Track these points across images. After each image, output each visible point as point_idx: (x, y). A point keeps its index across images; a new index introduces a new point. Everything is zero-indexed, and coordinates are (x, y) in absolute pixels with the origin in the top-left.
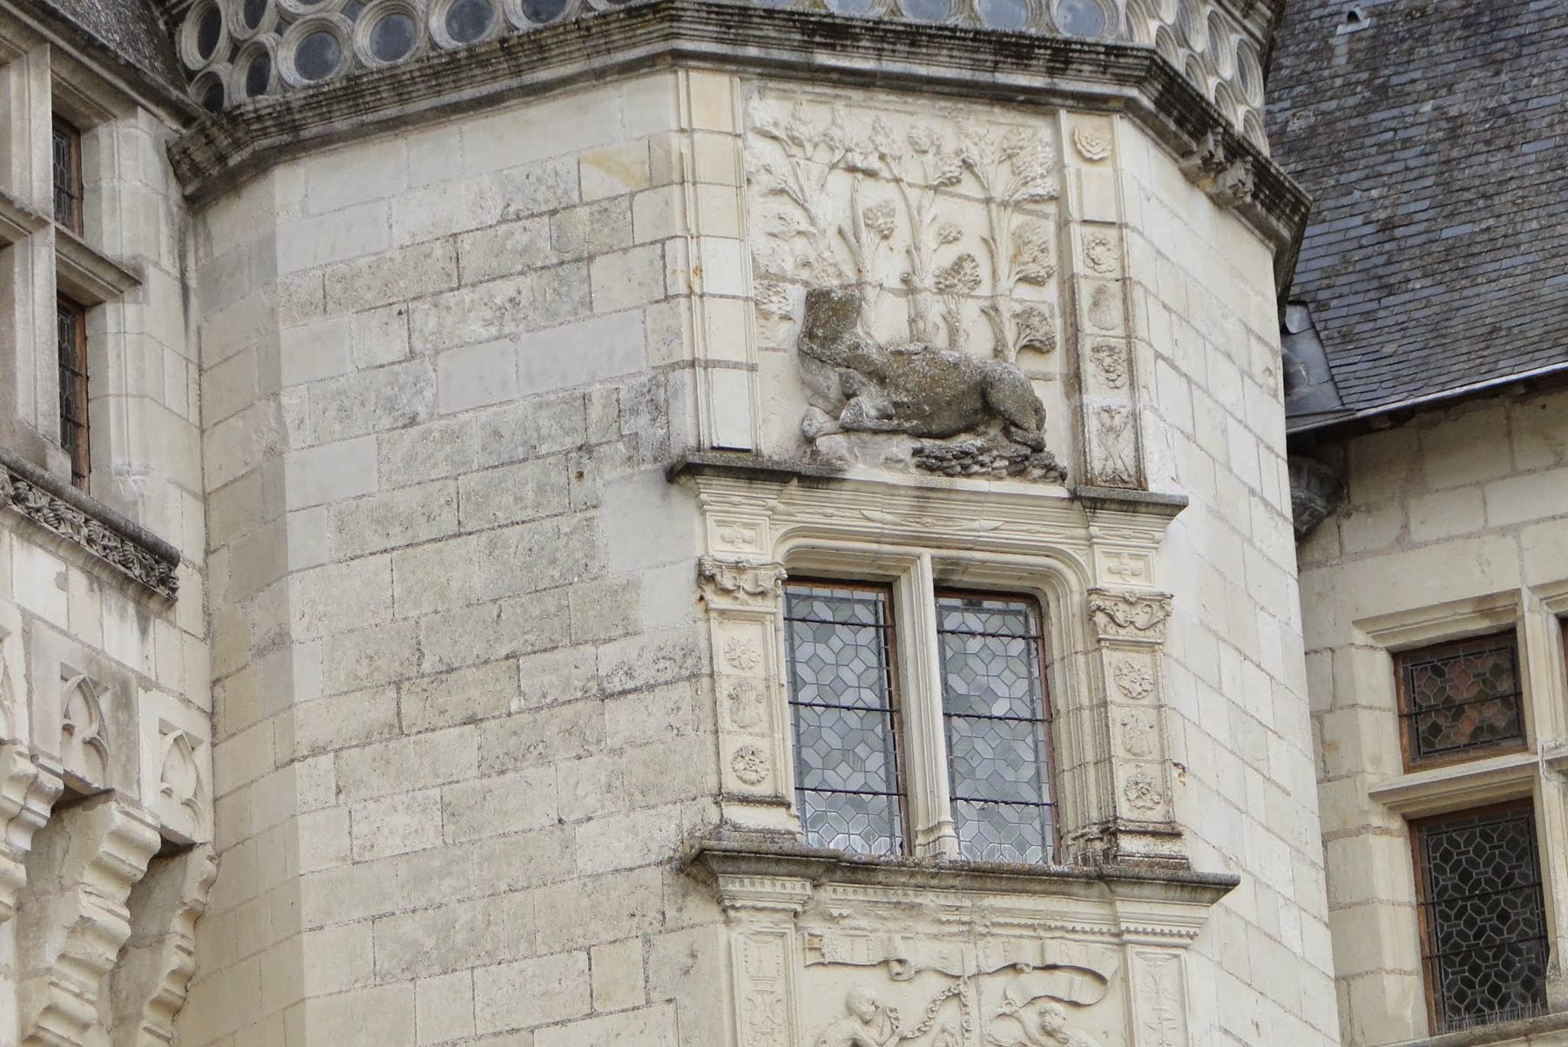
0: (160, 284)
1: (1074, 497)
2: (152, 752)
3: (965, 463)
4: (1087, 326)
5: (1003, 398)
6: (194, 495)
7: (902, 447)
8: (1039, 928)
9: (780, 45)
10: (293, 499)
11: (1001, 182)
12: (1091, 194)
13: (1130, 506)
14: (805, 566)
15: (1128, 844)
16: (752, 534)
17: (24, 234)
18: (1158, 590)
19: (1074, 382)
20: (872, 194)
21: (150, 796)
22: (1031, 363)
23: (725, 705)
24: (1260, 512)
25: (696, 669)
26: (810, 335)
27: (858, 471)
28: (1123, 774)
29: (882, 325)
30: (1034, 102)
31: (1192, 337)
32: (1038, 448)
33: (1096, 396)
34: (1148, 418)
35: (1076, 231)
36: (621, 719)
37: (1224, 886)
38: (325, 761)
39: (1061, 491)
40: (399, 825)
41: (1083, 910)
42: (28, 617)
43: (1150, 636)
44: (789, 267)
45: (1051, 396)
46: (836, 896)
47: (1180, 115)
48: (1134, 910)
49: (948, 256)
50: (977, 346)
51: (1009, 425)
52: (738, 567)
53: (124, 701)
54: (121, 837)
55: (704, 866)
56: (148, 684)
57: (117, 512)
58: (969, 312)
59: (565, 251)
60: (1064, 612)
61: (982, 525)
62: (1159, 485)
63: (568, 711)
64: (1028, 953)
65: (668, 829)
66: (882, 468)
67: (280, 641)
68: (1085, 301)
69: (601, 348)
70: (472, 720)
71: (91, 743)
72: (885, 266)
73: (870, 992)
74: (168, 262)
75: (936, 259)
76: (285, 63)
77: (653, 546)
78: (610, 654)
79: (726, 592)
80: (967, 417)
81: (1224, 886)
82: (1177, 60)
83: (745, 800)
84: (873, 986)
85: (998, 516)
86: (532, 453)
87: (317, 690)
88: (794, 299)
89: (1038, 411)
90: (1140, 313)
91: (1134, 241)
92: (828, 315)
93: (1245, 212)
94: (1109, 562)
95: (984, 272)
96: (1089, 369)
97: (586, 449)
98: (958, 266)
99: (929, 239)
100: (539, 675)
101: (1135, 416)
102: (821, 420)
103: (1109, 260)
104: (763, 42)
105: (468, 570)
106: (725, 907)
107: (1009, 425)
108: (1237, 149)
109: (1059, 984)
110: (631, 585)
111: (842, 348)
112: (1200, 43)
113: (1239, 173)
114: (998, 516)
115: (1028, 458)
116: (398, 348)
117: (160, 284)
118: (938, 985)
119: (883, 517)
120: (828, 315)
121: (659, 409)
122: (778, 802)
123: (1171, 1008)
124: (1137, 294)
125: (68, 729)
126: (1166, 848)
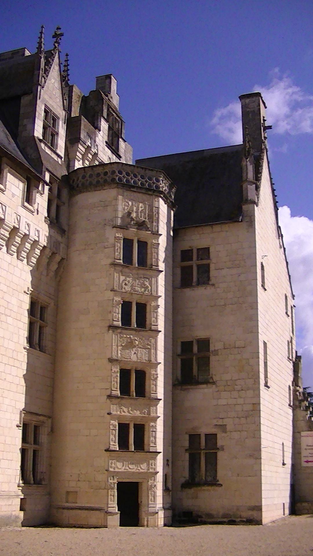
0: (66, 205)
13: (157, 234)
15: (154, 267)
78: (106, 244)
80: (141, 225)
85: (144, 235)
114: (144, 235)
115: (147, 229)
117: (66, 205)
121: (113, 221)
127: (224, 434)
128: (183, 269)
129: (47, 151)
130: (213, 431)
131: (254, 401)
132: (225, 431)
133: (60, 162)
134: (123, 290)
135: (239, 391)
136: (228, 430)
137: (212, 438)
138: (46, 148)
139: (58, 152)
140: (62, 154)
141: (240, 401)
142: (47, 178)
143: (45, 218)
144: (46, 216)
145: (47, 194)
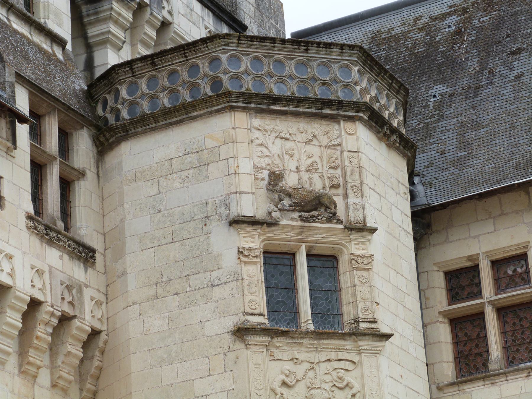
0: (91, 175)
1: (346, 227)
2: (88, 305)
3: (314, 219)
4: (349, 180)
5: (325, 201)
6: (101, 234)
7: (296, 215)
8: (337, 349)
10: (127, 234)
11: (325, 141)
12: (349, 143)
14: (271, 249)
15: (362, 325)
16: (254, 241)
17: (51, 162)
18: (370, 253)
19: (346, 196)
20: (289, 145)
21: (88, 317)
22: (333, 191)
23: (246, 288)
24: (403, 233)
25: (239, 279)
26: (269, 184)
27: (284, 222)
28: (360, 305)
29: (291, 181)
30: (334, 118)
31: (377, 183)
32: (335, 214)
33: (352, 199)
34: (367, 205)
35: (346, 154)
36: (217, 292)
37: (388, 336)
38: (136, 306)
39: (342, 226)
40: (157, 323)
41: (348, 344)
42: (51, 267)
44: (264, 165)
45: (339, 200)
46: (278, 341)
47: (377, 122)
48: (363, 343)
49: (309, 161)
50: (318, 187)
51: (327, 208)
52: (249, 249)
53: (80, 291)
54: (79, 329)
55: (241, 332)
56: (87, 286)
57: (77, 238)
58: (315, 177)
59: (201, 162)
60: (344, 262)
61: (319, 237)
62: (370, 224)
63: (203, 290)
64: (333, 355)
65: (230, 322)
66: (290, 221)
67: (124, 273)
68: (348, 173)
69: (211, 189)
70: (177, 294)
71: (71, 303)
72: (292, 165)
73: (288, 368)
74: (93, 169)
75: (306, 163)
76: (125, 114)
77: (227, 243)
78: (214, 274)
79: (246, 256)
80: (314, 206)
81: (388, 336)
82: (376, 106)
83: (252, 314)
84: (288, 366)
86: (192, 219)
87: (134, 285)
88: (266, 173)
89: (335, 205)
90: (364, 176)
91: (363, 157)
92: (275, 178)
93: (397, 149)
94: (355, 247)
96: (350, 192)
97: (207, 217)
98: (312, 164)
100: (195, 281)
101: (363, 205)
102: (272, 207)
103: (355, 161)
104: (255, 103)
105: (175, 252)
106: (247, 345)
107: (327, 208)
108: (394, 131)
109: (342, 364)
110: (220, 255)
111: (279, 188)
112: (383, 101)
113: (394, 137)
115: (333, 217)
116: (156, 191)
117: (91, 175)
118: (307, 365)
119: (290, 235)
120: (275, 178)
121: (227, 206)
122: (261, 315)
124: (364, 171)
125: (63, 299)
126: (373, 326)
128: (456, 322)
129: (15, 26)
133: (60, 56)
138: (12, 18)
139: (52, 26)
140: (64, 28)
142: (22, 102)
143: (29, 217)
144: (31, 210)
145: (28, 150)
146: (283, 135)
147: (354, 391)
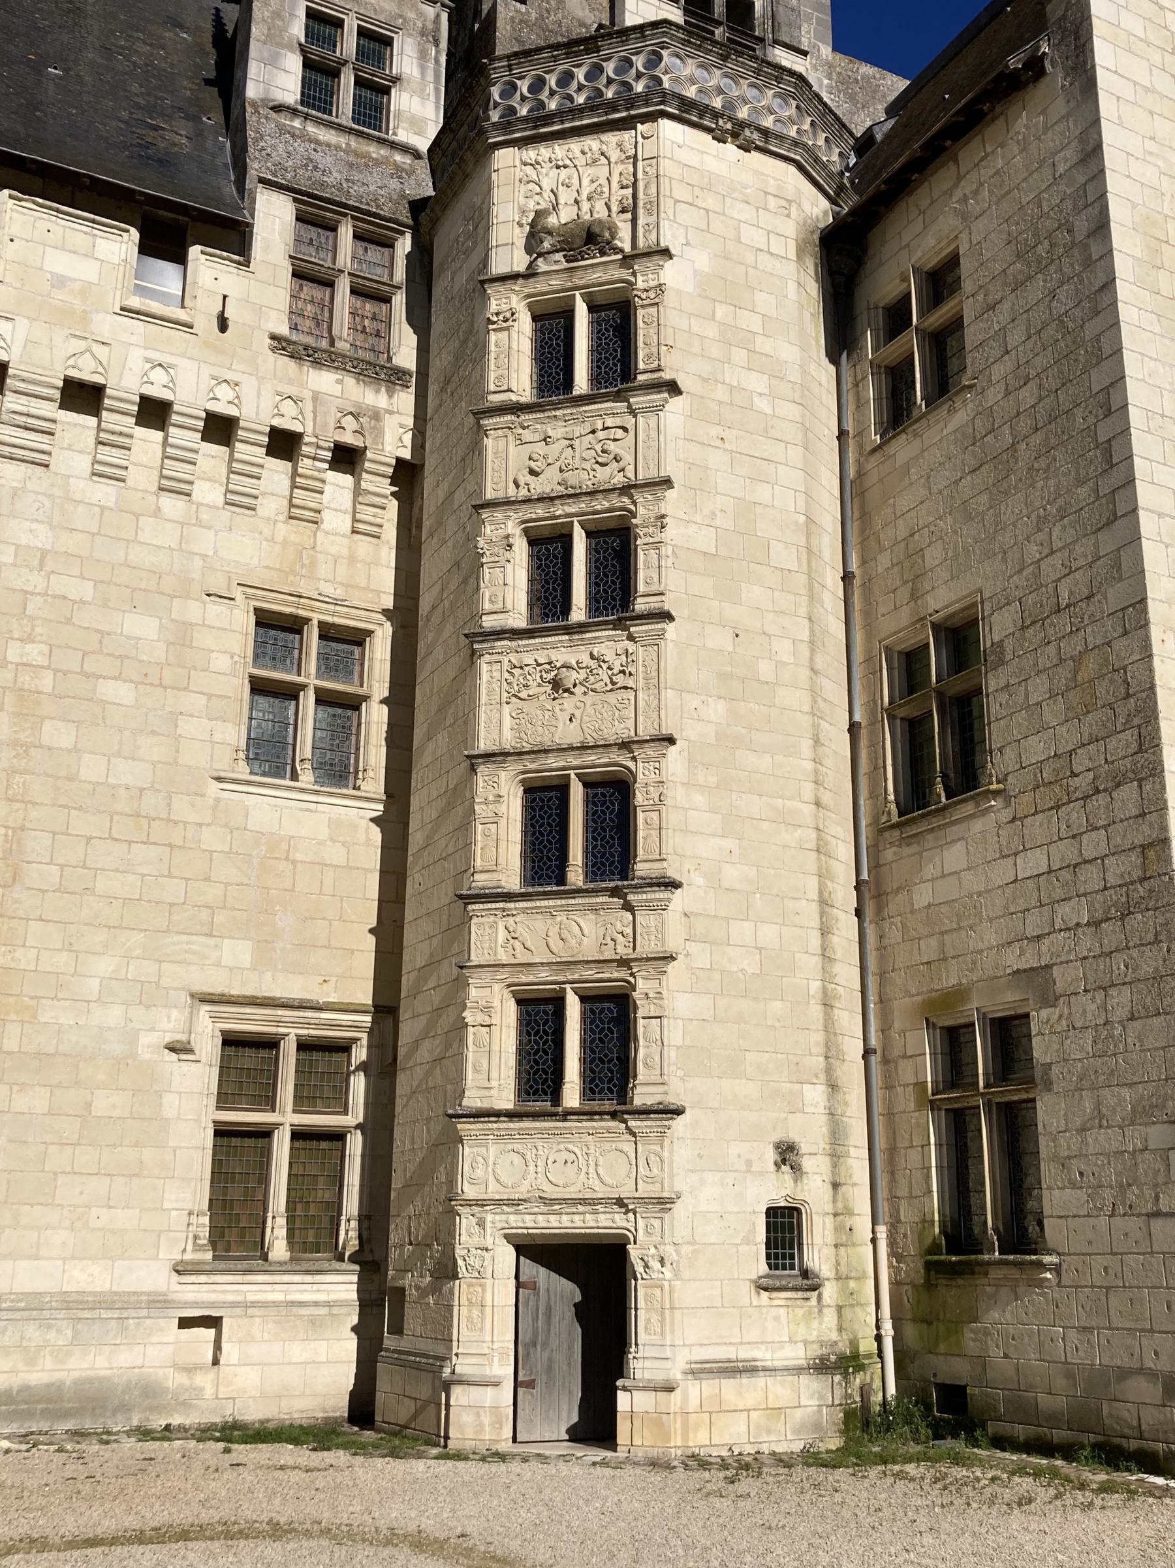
7: (559, 256)
9: (525, 129)
12: (646, 149)
20: (564, 173)
33: (641, 222)
43: (657, 300)
61: (597, 276)
72: (565, 196)
80: (589, 239)
84: (540, 448)
85: (601, 273)
95: (606, 190)
99: (585, 182)
114: (601, 273)
119: (556, 282)
123: (654, 434)
126: (656, 375)
127: (1044, 1013)
130: (1005, 1002)
131: (1143, 833)
132: (1049, 999)
134: (523, 493)
135: (1085, 798)
136: (1059, 987)
137: (1009, 1034)
141: (1094, 844)
146: (560, 163)
147: (622, 464)
